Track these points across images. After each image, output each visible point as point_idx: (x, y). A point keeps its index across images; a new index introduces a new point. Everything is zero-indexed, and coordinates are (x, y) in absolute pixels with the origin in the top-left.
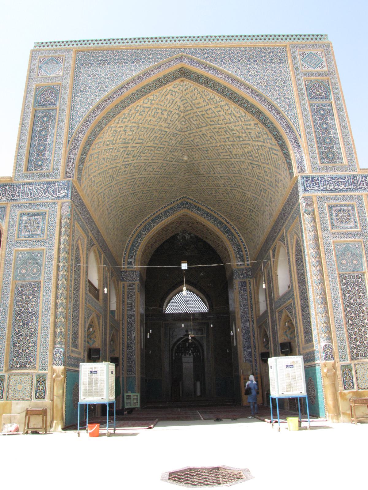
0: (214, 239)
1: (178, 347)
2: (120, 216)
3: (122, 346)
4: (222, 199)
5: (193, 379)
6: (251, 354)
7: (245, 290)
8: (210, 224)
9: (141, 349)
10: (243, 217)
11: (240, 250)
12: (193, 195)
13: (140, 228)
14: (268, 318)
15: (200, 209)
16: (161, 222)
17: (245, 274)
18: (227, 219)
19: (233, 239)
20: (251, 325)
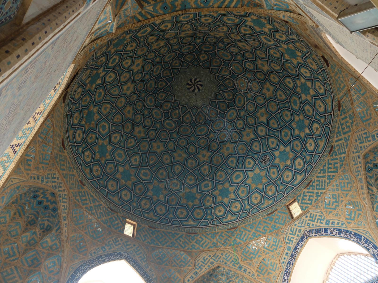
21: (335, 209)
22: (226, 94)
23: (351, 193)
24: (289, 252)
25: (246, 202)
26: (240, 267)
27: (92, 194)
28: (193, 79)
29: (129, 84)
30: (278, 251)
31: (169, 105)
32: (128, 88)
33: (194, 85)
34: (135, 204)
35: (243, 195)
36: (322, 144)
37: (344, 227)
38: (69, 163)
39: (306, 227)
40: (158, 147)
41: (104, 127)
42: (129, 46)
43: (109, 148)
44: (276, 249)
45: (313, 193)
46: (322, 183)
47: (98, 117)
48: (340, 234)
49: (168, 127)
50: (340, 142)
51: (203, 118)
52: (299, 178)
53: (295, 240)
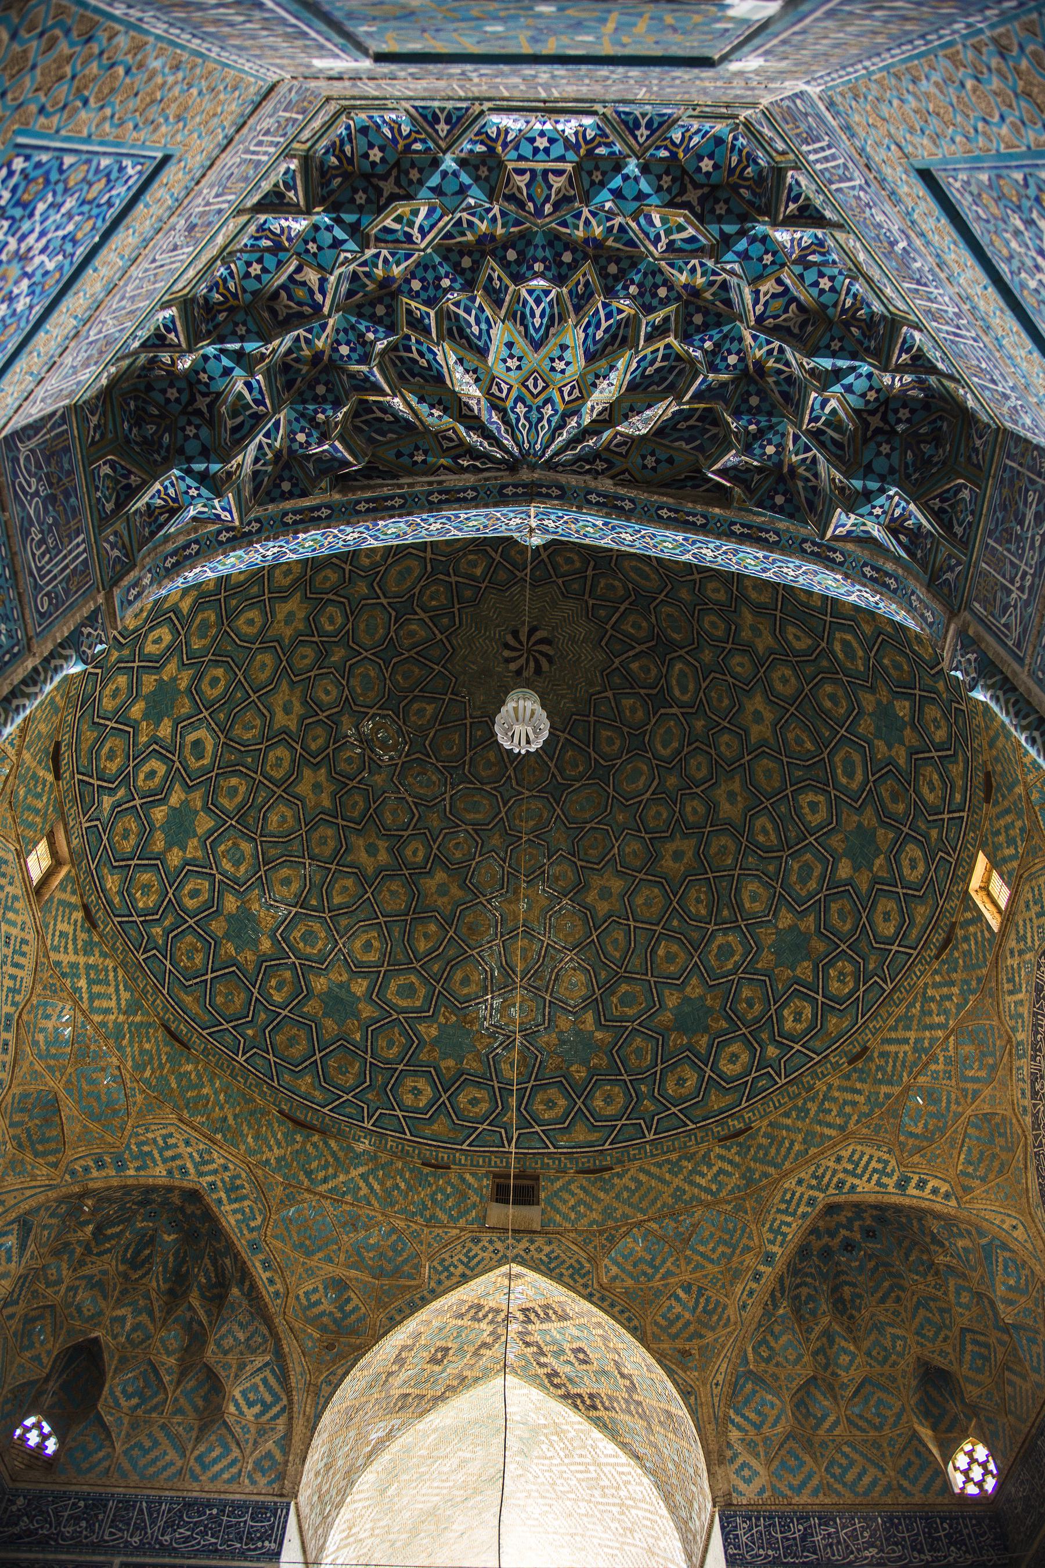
22: (478, 572)
27: (891, 1022)
28: (513, 666)
29: (591, 898)
31: (627, 702)
32: (605, 894)
33: (529, 651)
34: (934, 833)
38: (787, 1115)
40: (758, 717)
41: (726, 952)
42: (466, 991)
43: (786, 919)
47: (694, 981)
49: (691, 687)
51: (603, 582)
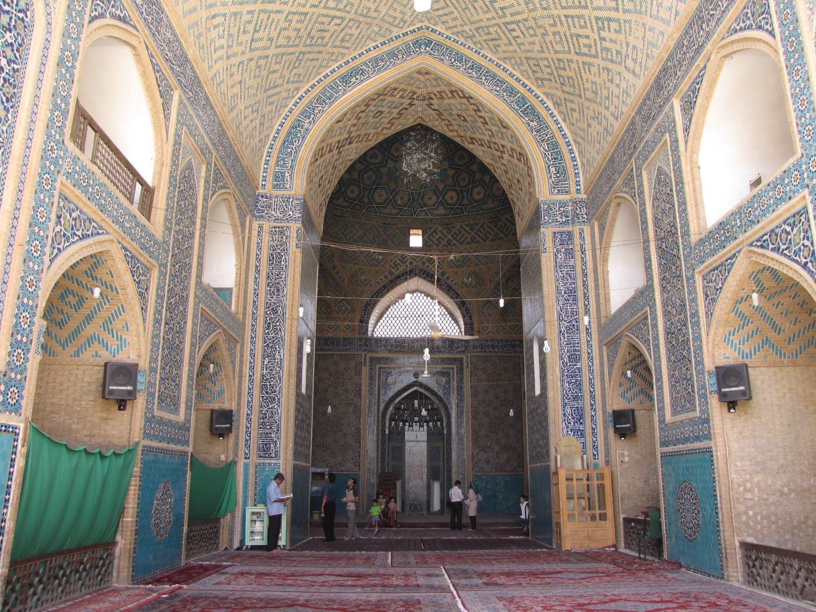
0: (492, 136)
1: (397, 409)
2: (251, 28)
3: (246, 384)
4: (519, 17)
5: (425, 477)
6: (581, 416)
7: (570, 253)
8: (483, 94)
9: (298, 394)
10: (575, 58)
11: (557, 157)
12: (444, 19)
13: (312, 95)
14: (653, 307)
15: (460, 58)
16: (364, 84)
17: (570, 214)
18: (527, 82)
19: (541, 129)
20: (584, 341)
21: (458, 267)
23: (482, 266)
24: (389, 276)
25: (366, 193)
26: (334, 267)
30: (377, 268)
35: (368, 183)
36: (490, 205)
37: (455, 287)
39: (420, 263)
44: (376, 266)
45: (446, 237)
46: (462, 236)
48: (448, 290)
50: (510, 224)
52: (441, 211)
53: (401, 269)
